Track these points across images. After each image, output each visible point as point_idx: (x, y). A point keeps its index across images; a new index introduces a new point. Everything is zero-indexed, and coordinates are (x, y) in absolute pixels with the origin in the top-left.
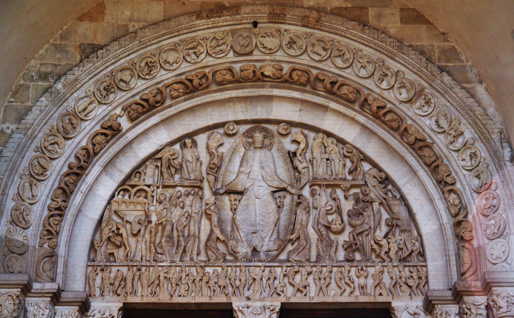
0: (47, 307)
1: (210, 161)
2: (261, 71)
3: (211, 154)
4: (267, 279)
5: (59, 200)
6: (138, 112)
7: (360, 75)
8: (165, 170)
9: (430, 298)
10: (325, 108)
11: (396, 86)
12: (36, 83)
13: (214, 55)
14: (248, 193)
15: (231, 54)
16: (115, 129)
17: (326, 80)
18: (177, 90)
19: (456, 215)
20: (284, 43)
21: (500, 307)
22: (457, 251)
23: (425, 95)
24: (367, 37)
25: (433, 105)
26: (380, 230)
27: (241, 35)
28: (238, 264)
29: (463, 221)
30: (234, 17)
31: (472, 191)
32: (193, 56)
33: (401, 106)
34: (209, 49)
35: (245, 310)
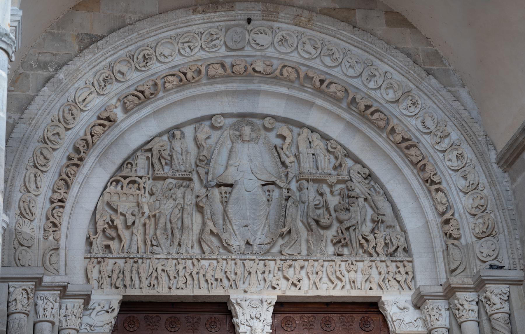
0: (57, 301)
1: (198, 153)
3: (199, 146)
5: (62, 191)
7: (348, 74)
8: (157, 161)
9: (422, 294)
10: (311, 104)
11: (384, 86)
12: (35, 72)
13: (207, 49)
15: (223, 49)
17: (315, 78)
18: (172, 83)
19: (443, 214)
20: (276, 40)
21: (494, 304)
24: (357, 38)
25: (419, 106)
26: (366, 225)
28: (233, 257)
29: (451, 219)
30: (229, 13)
31: (459, 191)
32: (188, 50)
33: (387, 105)
34: (202, 43)
35: (243, 303)
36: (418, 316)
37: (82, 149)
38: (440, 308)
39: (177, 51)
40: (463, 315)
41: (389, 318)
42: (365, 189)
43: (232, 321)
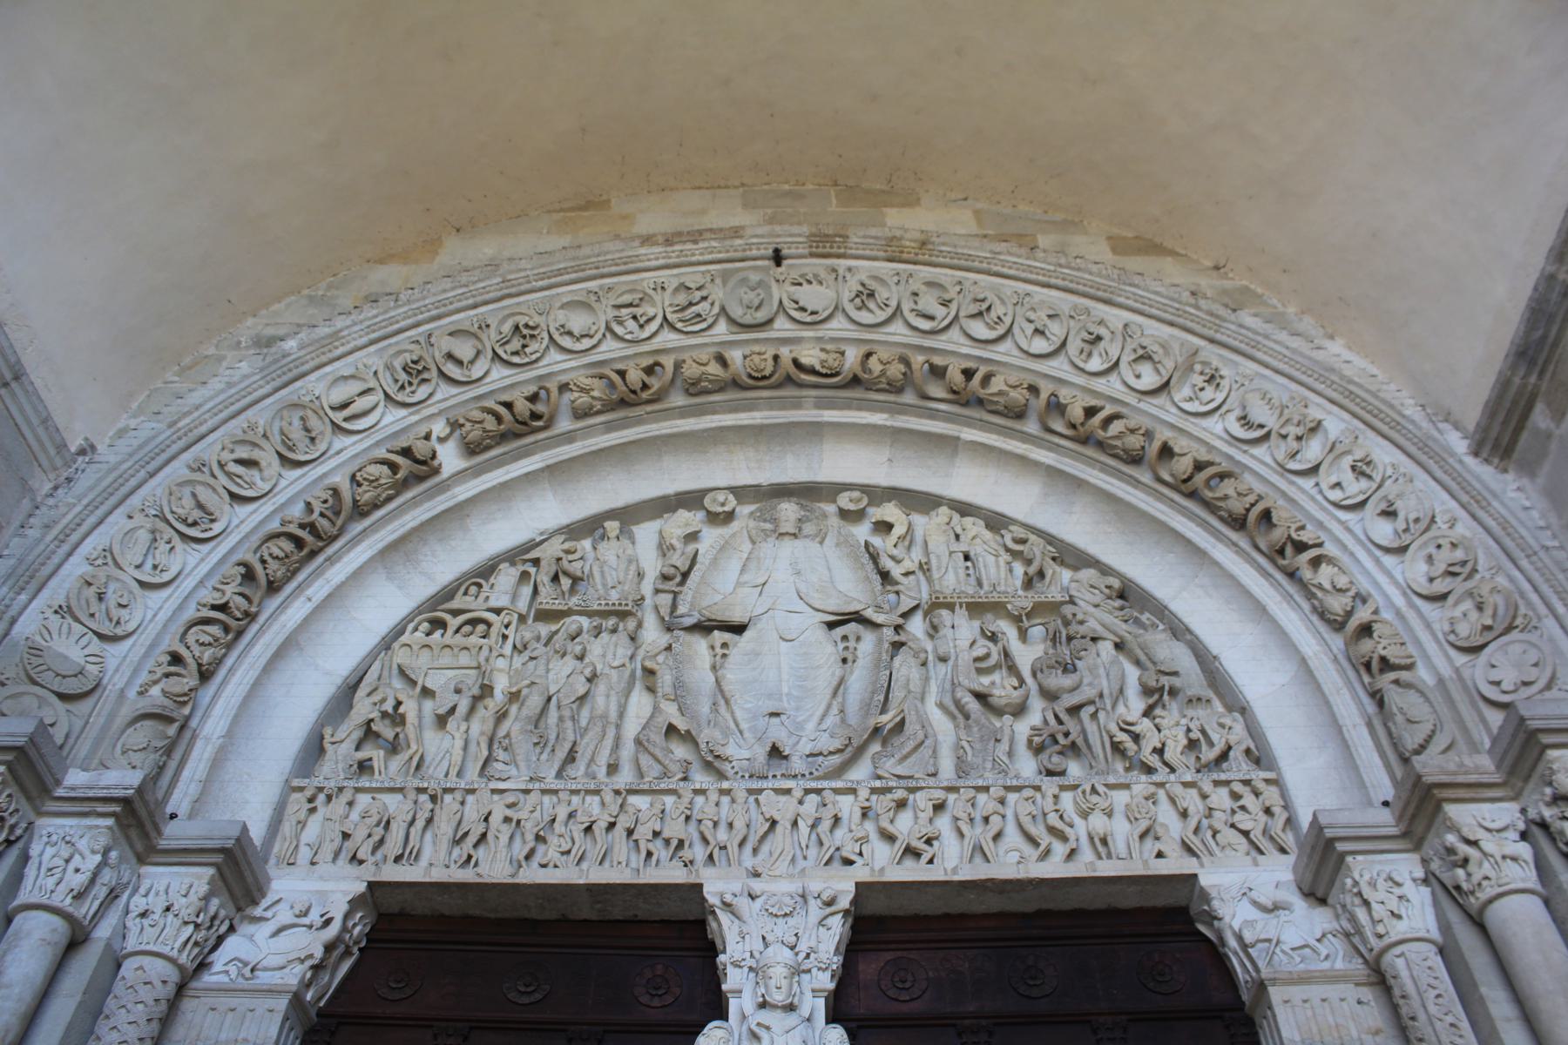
2: (794, 355)
3: (664, 549)
4: (810, 822)
6: (485, 430)
7: (1032, 351)
9: (1329, 833)
11: (1125, 360)
13: (679, 325)
14: (759, 626)
15: (722, 327)
16: (419, 456)
17: (950, 368)
20: (847, 295)
22: (1371, 708)
23: (1204, 363)
24: (1043, 266)
25: (1225, 383)
26: (1126, 706)
27: (744, 281)
28: (726, 785)
29: (1375, 621)
30: (728, 243)
31: (1378, 553)
32: (631, 324)
33: (1142, 405)
34: (668, 310)
35: (743, 903)
36: (1328, 926)
37: (318, 507)
38: (1397, 879)
39: (603, 326)
40: (1487, 878)
41: (1232, 942)
42: (1116, 621)
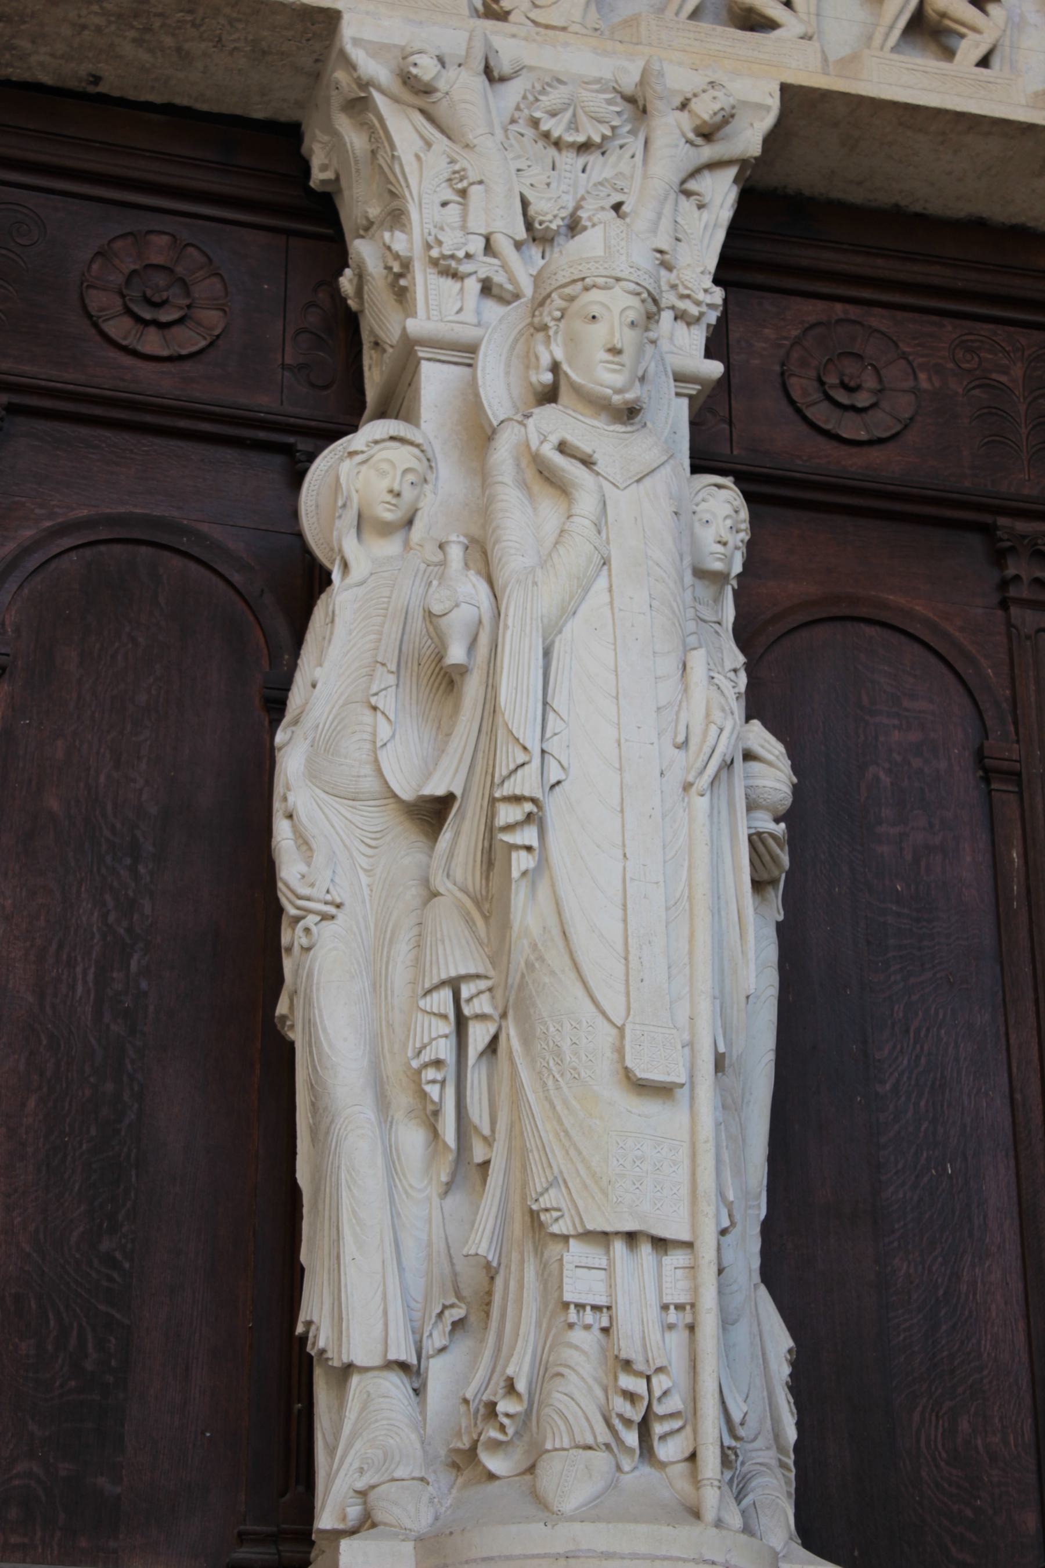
43: (346, 282)
